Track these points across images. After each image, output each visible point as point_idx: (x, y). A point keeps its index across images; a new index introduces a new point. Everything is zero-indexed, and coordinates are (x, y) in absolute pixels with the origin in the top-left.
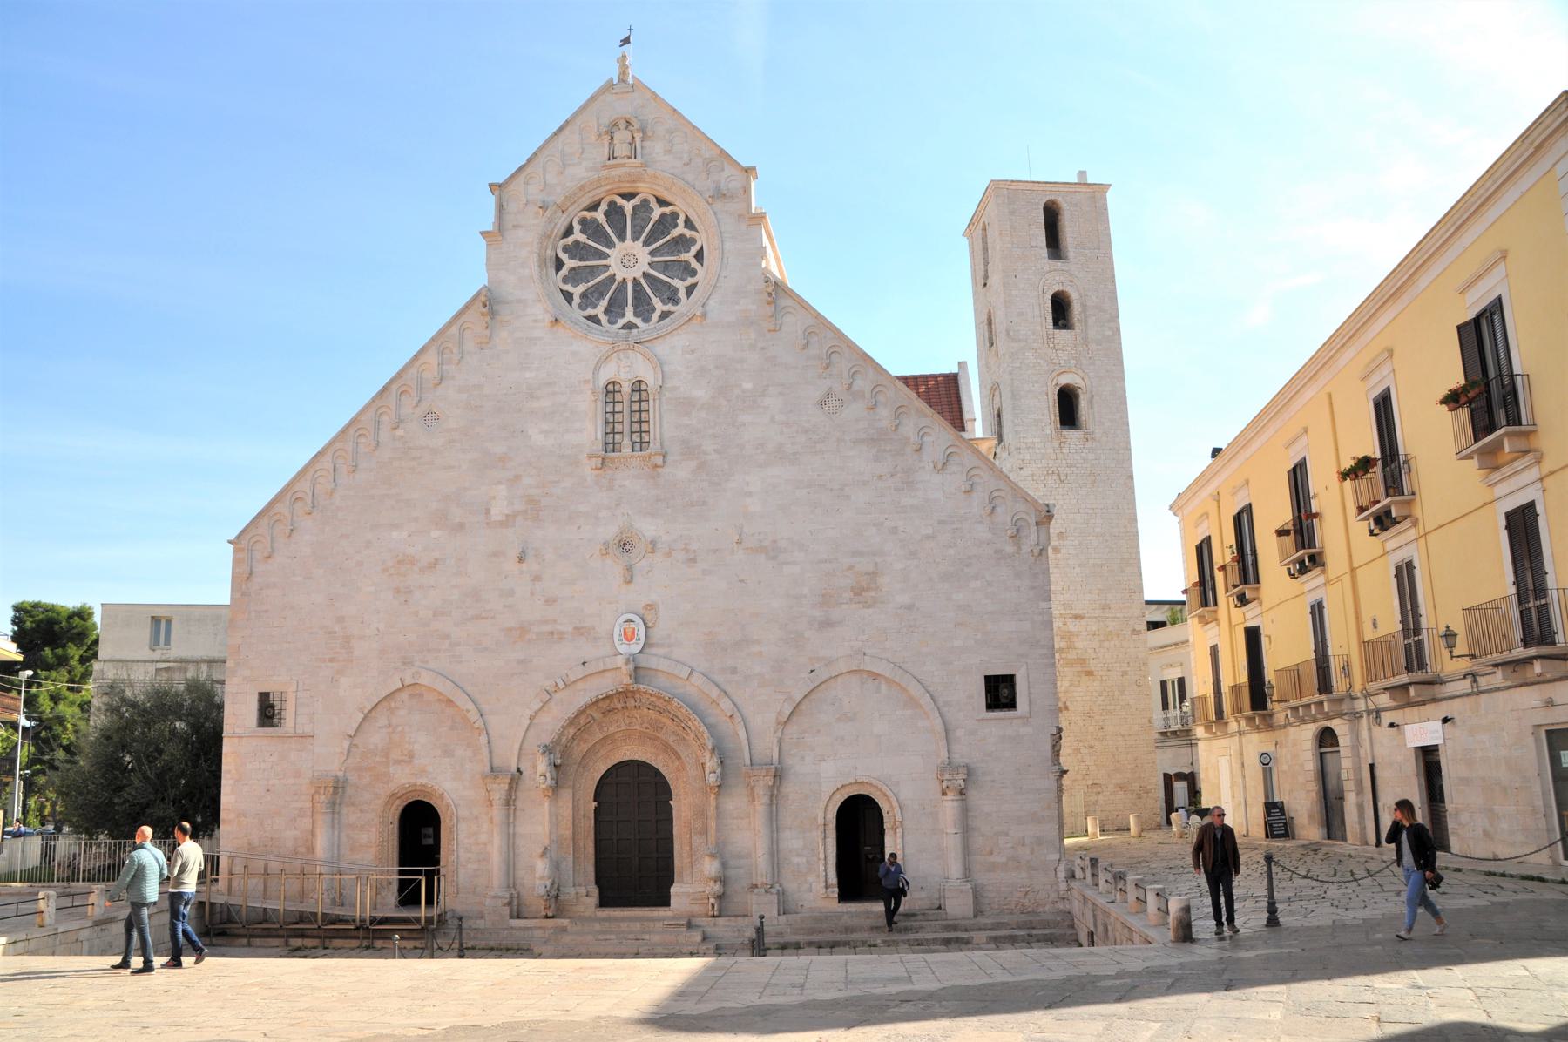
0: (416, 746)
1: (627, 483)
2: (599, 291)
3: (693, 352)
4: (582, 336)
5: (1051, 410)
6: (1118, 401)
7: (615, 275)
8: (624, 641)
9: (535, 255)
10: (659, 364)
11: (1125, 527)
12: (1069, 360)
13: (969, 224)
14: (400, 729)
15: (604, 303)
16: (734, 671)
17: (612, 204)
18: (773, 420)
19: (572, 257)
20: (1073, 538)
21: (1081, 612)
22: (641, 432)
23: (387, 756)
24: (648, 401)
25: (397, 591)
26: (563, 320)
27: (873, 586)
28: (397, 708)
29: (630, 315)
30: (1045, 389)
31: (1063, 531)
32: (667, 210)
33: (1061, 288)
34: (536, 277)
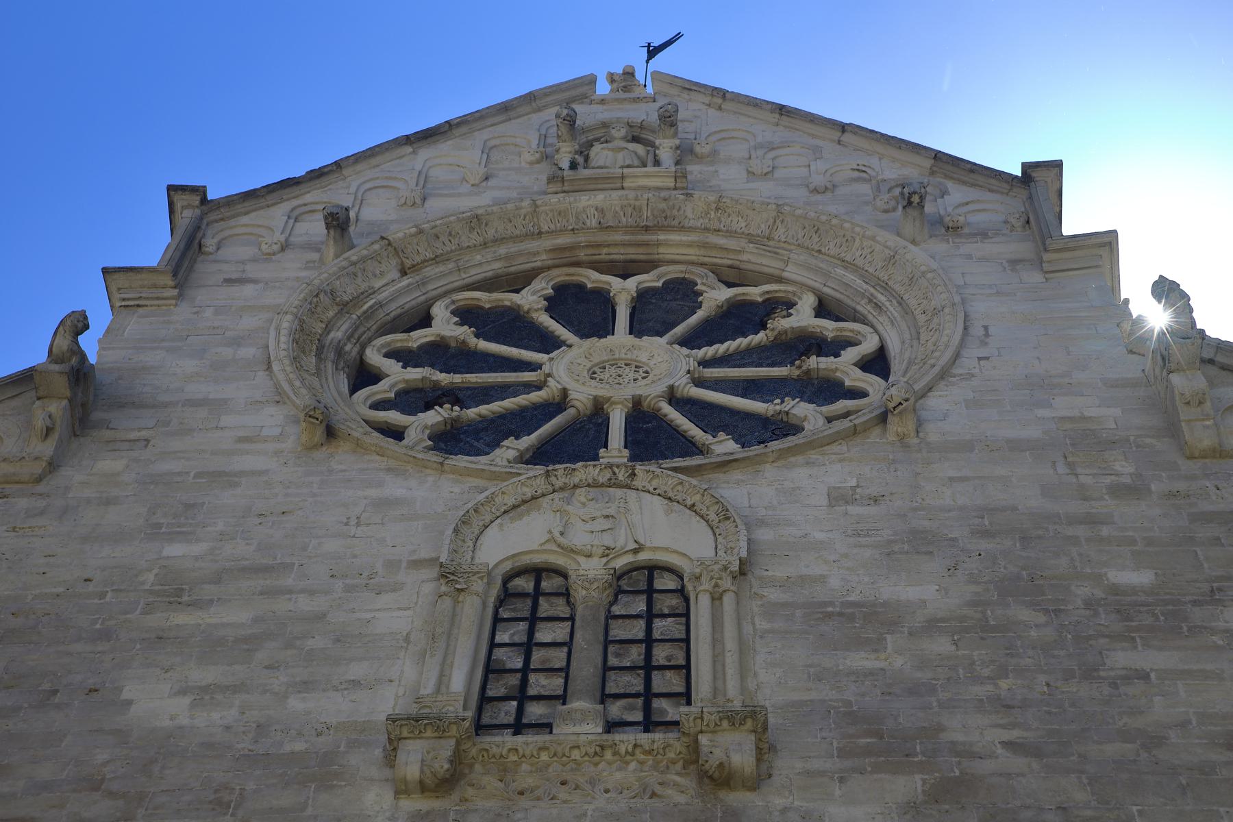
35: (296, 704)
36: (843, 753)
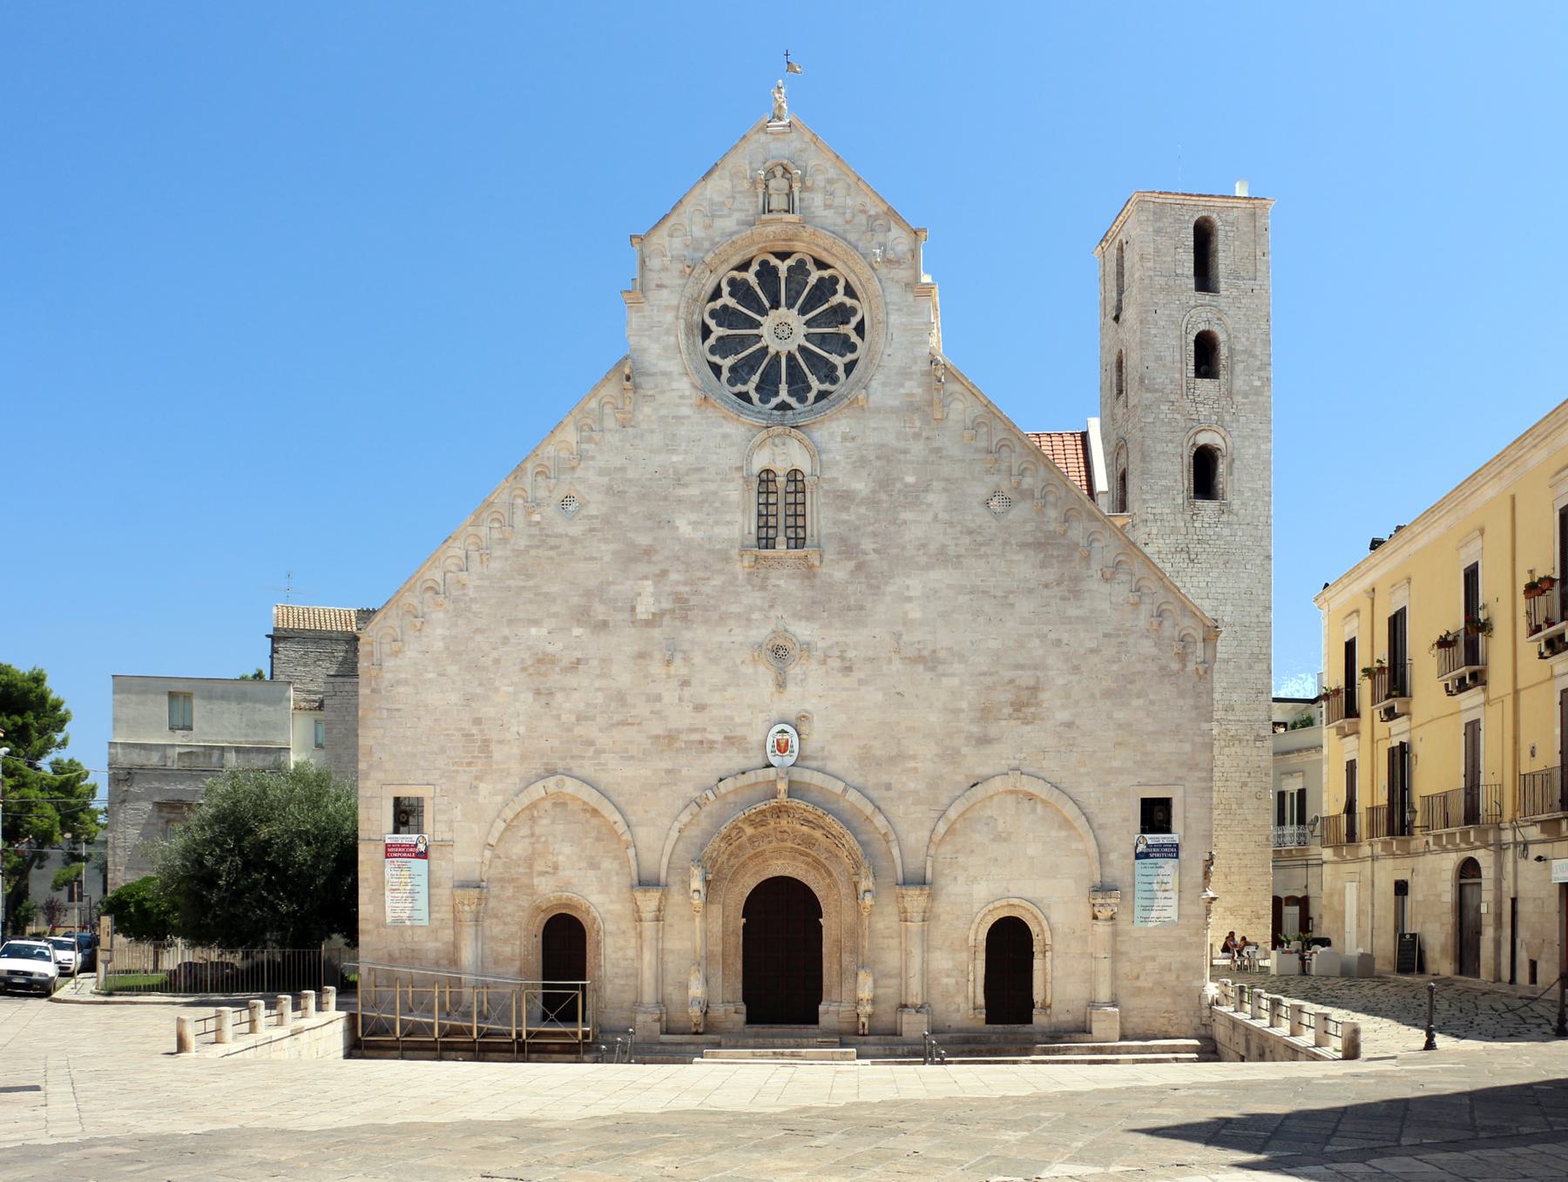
0: (561, 858)
1: (781, 582)
2: (749, 365)
3: (853, 439)
4: (732, 418)
5: (1185, 474)
6: (1261, 467)
7: (767, 347)
8: (777, 753)
9: (682, 321)
10: (815, 452)
12: (1210, 415)
13: (1102, 240)
14: (543, 839)
15: (756, 378)
16: (888, 787)
17: (764, 264)
18: (936, 517)
19: (719, 324)
22: (796, 527)
23: (531, 867)
24: (804, 492)
25: (538, 692)
26: (712, 398)
27: (1033, 701)
28: (541, 817)
29: (784, 394)
30: (1180, 449)
32: (826, 274)
33: (1207, 328)
34: (683, 347)
35: (717, 530)
36: (839, 553)
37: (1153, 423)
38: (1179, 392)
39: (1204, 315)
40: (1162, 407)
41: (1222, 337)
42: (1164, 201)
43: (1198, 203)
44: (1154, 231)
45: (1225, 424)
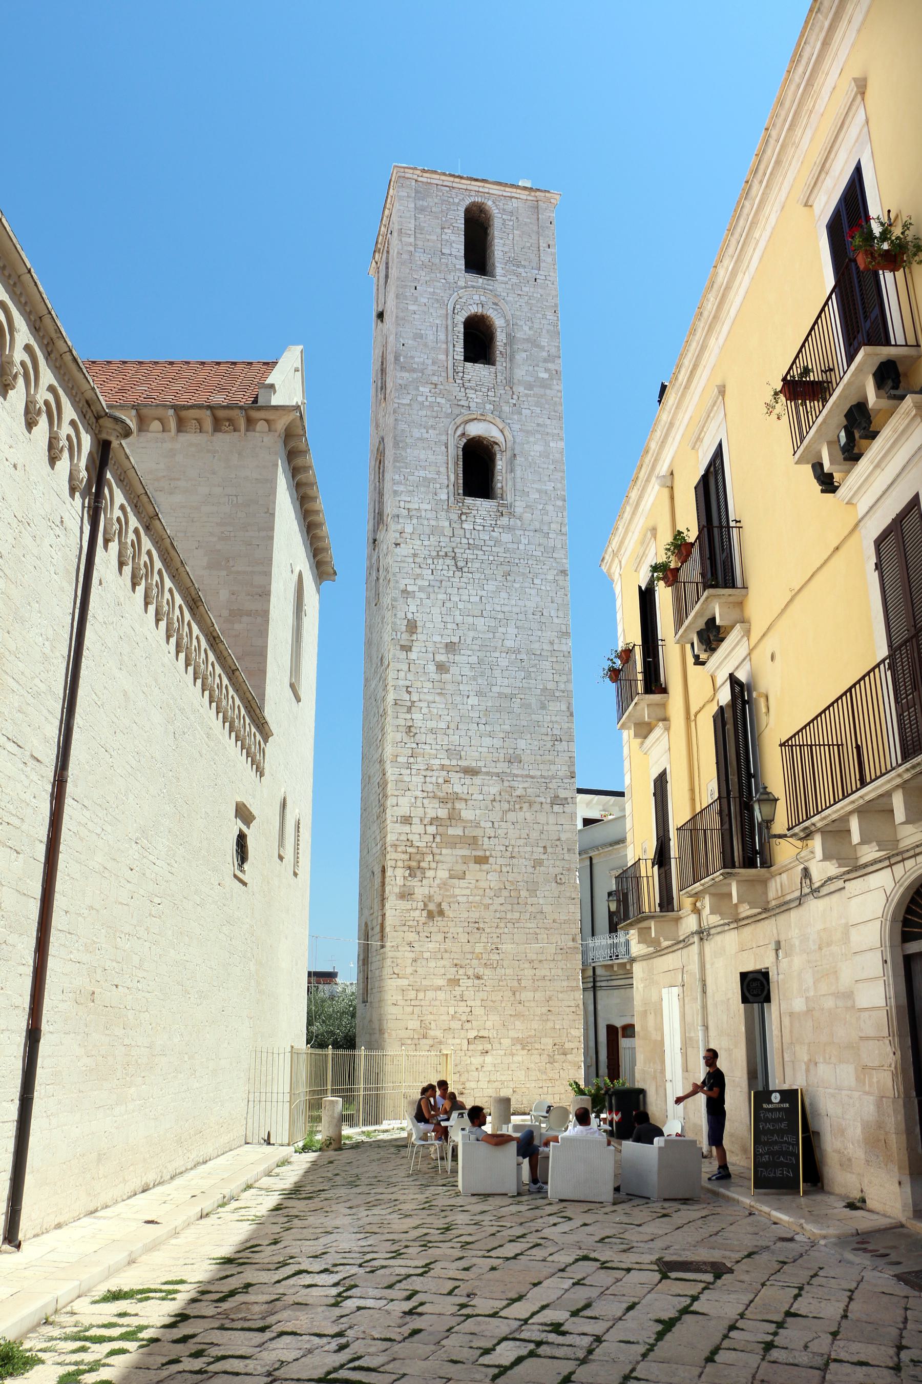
5: (451, 466)
6: (552, 467)
11: (552, 643)
12: (484, 403)
20: (470, 653)
21: (474, 764)
30: (444, 438)
31: (456, 639)
37: (410, 405)
38: (444, 374)
39: (476, 297)
40: (421, 389)
41: (498, 323)
42: (429, 181)
43: (469, 187)
44: (416, 208)
45: (504, 416)
